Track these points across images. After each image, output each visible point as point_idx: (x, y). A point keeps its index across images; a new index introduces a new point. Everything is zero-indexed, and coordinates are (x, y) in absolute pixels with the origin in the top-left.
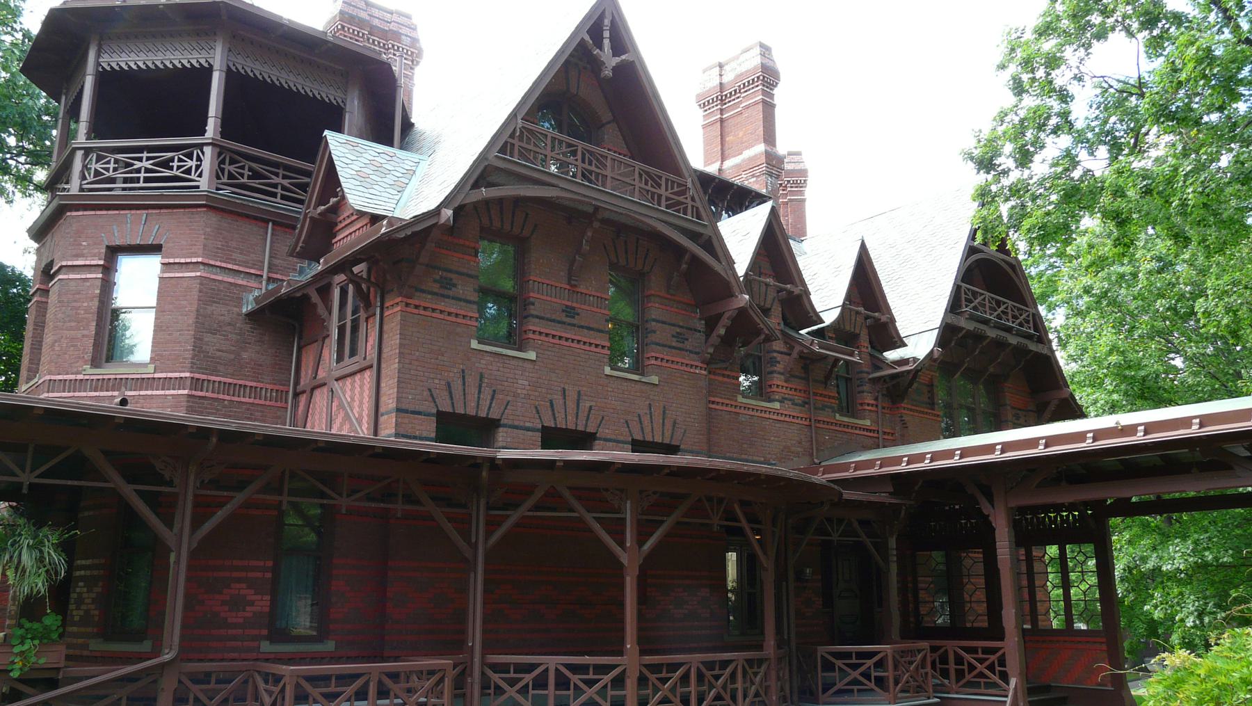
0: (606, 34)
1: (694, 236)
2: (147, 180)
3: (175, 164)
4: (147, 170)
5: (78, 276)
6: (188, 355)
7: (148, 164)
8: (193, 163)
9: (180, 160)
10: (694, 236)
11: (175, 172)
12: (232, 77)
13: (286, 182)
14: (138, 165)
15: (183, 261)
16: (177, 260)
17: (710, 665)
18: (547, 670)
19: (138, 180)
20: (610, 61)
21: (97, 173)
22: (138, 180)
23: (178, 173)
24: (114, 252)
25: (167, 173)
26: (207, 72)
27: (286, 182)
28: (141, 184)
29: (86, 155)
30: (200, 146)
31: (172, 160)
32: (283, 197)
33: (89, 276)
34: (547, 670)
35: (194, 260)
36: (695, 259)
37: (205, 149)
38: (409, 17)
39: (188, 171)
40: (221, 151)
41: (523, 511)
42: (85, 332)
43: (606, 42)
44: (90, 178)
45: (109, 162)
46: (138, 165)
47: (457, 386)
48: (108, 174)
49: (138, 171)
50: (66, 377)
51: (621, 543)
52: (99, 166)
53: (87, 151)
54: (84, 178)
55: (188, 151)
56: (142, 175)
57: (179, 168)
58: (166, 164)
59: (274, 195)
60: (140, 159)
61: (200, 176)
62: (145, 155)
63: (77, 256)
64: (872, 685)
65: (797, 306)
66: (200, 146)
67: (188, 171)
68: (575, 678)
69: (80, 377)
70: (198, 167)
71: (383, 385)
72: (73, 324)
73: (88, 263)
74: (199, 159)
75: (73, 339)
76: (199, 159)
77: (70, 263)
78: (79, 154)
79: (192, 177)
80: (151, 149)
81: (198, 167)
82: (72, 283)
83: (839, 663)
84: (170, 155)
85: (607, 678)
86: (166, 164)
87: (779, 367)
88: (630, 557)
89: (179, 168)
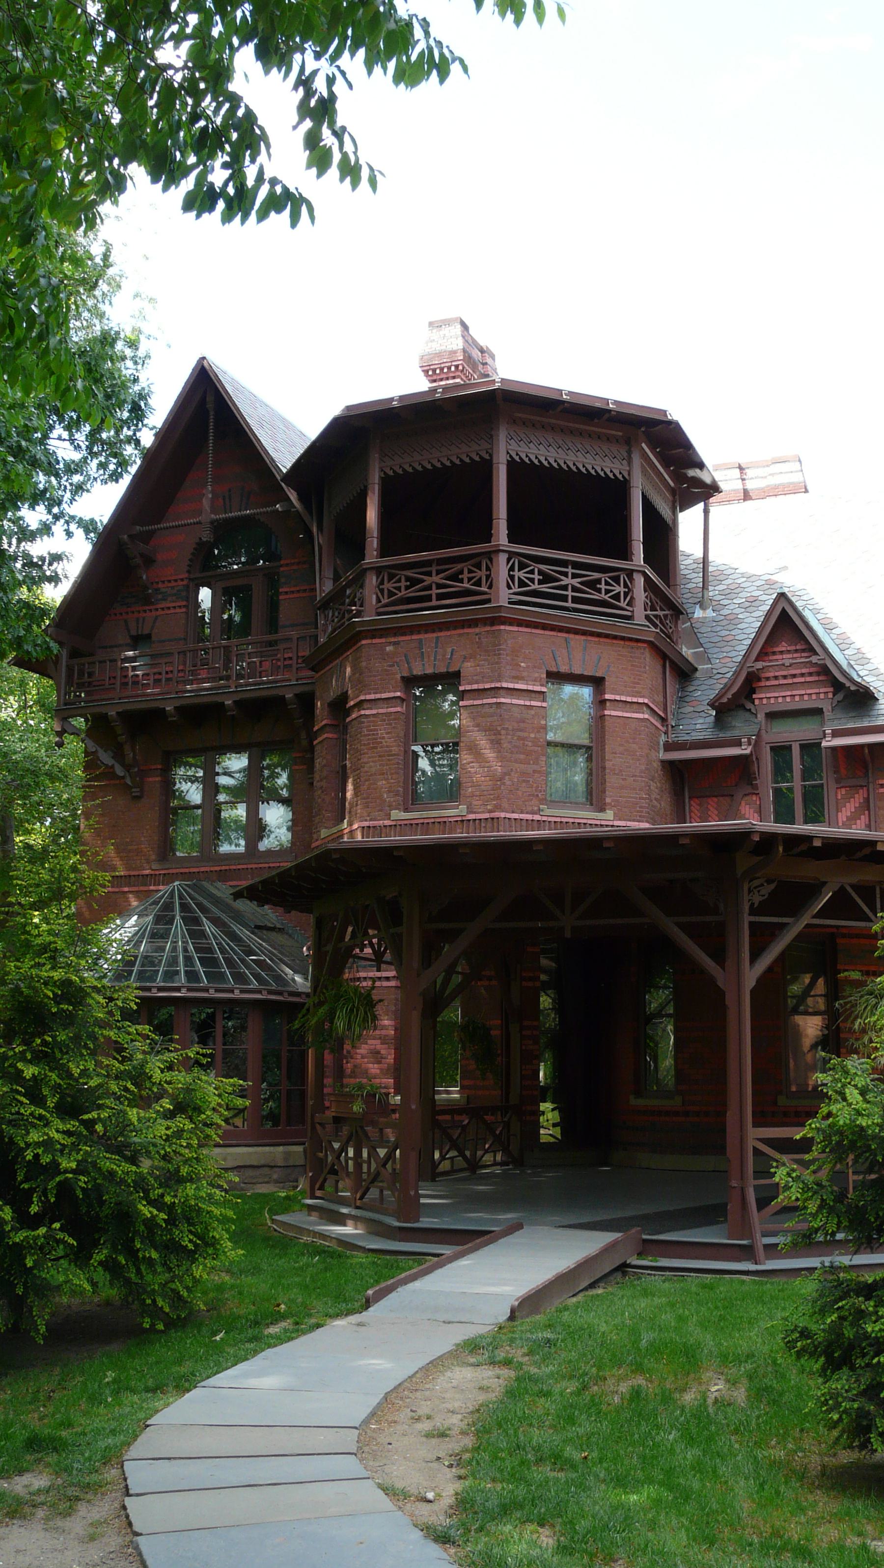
2: (575, 600)
3: (603, 587)
4: (575, 589)
5: (522, 702)
6: (644, 803)
7: (575, 582)
8: (620, 589)
9: (607, 583)
11: (604, 596)
14: (565, 581)
15: (629, 699)
16: (623, 698)
19: (564, 598)
21: (522, 584)
22: (564, 598)
24: (558, 677)
25: (596, 596)
28: (569, 604)
29: (508, 560)
30: (630, 573)
31: (599, 581)
33: (533, 703)
35: (641, 700)
37: (636, 576)
38: (493, 357)
42: (535, 767)
45: (532, 572)
48: (533, 587)
49: (565, 588)
50: (522, 816)
53: (511, 555)
54: (509, 587)
55: (615, 575)
57: (607, 592)
58: (593, 585)
62: (570, 570)
63: (517, 678)
66: (630, 573)
67: (617, 597)
69: (537, 817)
70: (626, 594)
72: (522, 757)
73: (530, 688)
75: (523, 774)
76: (626, 586)
77: (511, 686)
78: (503, 558)
79: (623, 604)
80: (576, 565)
81: (626, 594)
82: (514, 709)
86: (593, 585)
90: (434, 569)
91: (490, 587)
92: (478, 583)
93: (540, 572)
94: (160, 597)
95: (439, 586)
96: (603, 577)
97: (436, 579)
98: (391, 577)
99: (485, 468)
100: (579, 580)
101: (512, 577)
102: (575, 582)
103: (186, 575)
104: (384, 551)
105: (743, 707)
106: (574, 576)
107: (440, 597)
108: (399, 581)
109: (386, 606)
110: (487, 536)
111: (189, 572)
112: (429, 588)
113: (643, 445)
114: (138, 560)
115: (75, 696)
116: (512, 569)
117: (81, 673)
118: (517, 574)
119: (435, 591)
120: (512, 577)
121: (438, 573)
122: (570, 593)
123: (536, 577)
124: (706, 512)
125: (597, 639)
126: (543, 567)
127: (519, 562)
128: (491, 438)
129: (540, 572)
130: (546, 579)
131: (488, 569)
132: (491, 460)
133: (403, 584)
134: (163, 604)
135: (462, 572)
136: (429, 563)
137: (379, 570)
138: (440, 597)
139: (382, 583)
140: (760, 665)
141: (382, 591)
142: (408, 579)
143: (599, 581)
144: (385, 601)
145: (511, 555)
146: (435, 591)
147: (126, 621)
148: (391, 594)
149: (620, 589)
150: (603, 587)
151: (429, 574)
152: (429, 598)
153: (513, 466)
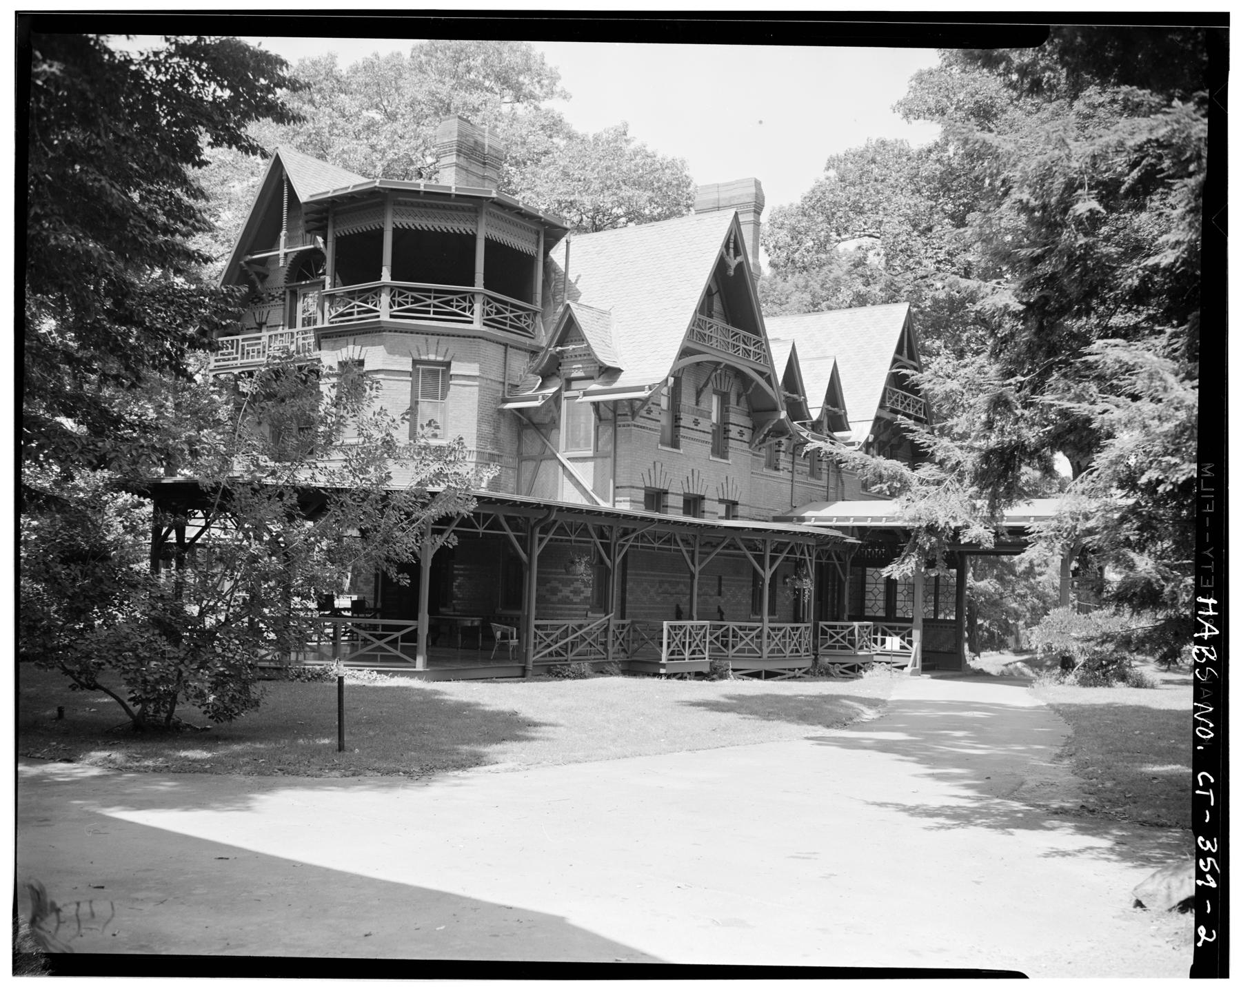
0: (732, 245)
1: (761, 374)
2: (435, 313)
3: (455, 304)
4: (435, 306)
7: (435, 302)
8: (467, 304)
10: (761, 374)
12: (491, 245)
13: (511, 315)
14: (429, 301)
17: (793, 629)
18: (728, 630)
19: (428, 312)
20: (733, 262)
25: (449, 309)
26: (473, 238)
27: (511, 315)
28: (431, 316)
30: (473, 295)
32: (511, 326)
34: (728, 630)
36: (758, 385)
40: (489, 300)
41: (719, 550)
43: (732, 251)
44: (396, 308)
46: (429, 301)
47: (652, 472)
49: (429, 306)
51: (764, 569)
53: (392, 289)
56: (432, 310)
59: (505, 324)
60: (429, 297)
62: (432, 295)
64: (846, 643)
65: (797, 410)
68: (741, 633)
71: (618, 470)
78: (388, 290)
79: (468, 314)
80: (437, 291)
83: (830, 631)
84: (450, 297)
85: (754, 633)
86: (448, 303)
87: (783, 448)
88: (767, 575)
95: (359, 306)
96: (455, 297)
99: (379, 234)
102: (435, 302)
105: (553, 374)
106: (435, 298)
107: (359, 313)
110: (379, 277)
114: (254, 276)
119: (356, 310)
123: (410, 300)
126: (415, 294)
128: (383, 215)
130: (416, 300)
134: (273, 303)
138: (359, 313)
140: (559, 348)
146: (356, 310)
150: (455, 304)
152: (351, 314)
153: (398, 233)
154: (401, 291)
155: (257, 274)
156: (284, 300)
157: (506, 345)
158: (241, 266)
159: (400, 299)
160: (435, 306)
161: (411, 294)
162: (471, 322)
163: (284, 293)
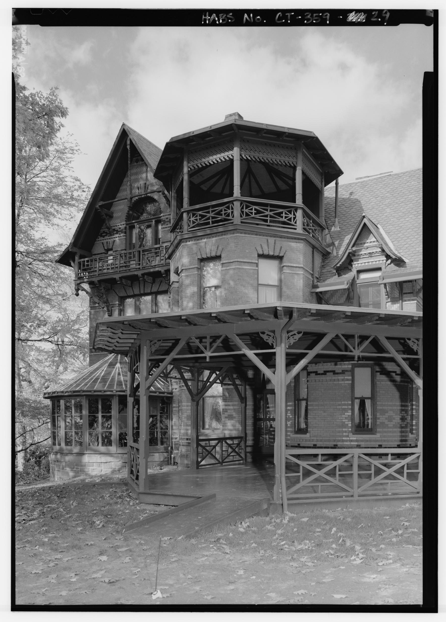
3: (284, 215)
4: (271, 217)
7: (271, 213)
8: (292, 216)
11: (284, 219)
14: (267, 213)
21: (247, 215)
23: (285, 220)
25: (281, 219)
31: (282, 213)
39: (290, 220)
49: (267, 216)
52: (247, 211)
53: (242, 202)
54: (241, 216)
55: (290, 210)
58: (279, 214)
60: (267, 210)
61: (296, 223)
62: (269, 208)
67: (290, 220)
70: (294, 218)
74: (294, 214)
76: (294, 214)
79: (292, 223)
80: (272, 206)
84: (281, 210)
89: (286, 217)
90: (211, 210)
91: (233, 217)
92: (228, 215)
93: (255, 209)
94: (115, 232)
97: (212, 215)
98: (193, 215)
100: (273, 212)
101: (243, 212)
102: (271, 213)
103: (124, 223)
104: (191, 203)
108: (197, 216)
109: (193, 227)
110: (231, 194)
111: (125, 221)
112: (208, 219)
113: (304, 150)
114: (104, 216)
115: (83, 274)
116: (243, 208)
117: (84, 265)
118: (244, 210)
120: (243, 212)
121: (212, 211)
122: (269, 218)
123: (254, 211)
124: (337, 184)
125: (281, 239)
126: (257, 207)
127: (246, 205)
129: (255, 209)
130: (258, 212)
131: (232, 209)
132: (233, 159)
133: (198, 218)
135: (221, 211)
136: (208, 208)
137: (188, 212)
138: (213, 222)
139: (190, 218)
141: (190, 221)
142: (200, 215)
143: (282, 213)
144: (192, 226)
145: (242, 202)
146: (210, 221)
147: (103, 243)
148: (194, 222)
149: (292, 216)
151: (208, 212)
152: (208, 223)
154: (248, 204)
155: (107, 215)
156: (125, 233)
157: (314, 247)
158: (96, 210)
159: (247, 211)
160: (271, 217)
161: (254, 207)
162: (295, 229)
163: (126, 228)
